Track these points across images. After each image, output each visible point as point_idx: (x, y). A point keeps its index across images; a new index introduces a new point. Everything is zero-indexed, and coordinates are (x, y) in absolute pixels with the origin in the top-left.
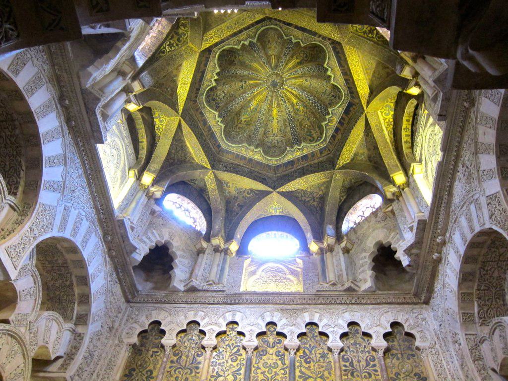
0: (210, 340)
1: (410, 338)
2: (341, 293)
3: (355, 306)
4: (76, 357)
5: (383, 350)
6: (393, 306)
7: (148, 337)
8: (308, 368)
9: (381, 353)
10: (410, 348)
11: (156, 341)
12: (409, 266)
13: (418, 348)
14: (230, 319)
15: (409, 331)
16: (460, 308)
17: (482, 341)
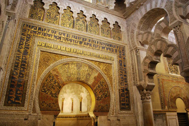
0: (61, 11)
1: (119, 27)
2: (104, 8)
3: (107, 13)
4: (17, 6)
5: (112, 29)
6: (117, 17)
7: (37, 3)
8: (92, 28)
9: (111, 29)
10: (118, 30)
11: (41, 6)
12: (128, 7)
13: (120, 31)
14: (68, 5)
15: (120, 25)
16: (139, 25)
17: (139, 34)
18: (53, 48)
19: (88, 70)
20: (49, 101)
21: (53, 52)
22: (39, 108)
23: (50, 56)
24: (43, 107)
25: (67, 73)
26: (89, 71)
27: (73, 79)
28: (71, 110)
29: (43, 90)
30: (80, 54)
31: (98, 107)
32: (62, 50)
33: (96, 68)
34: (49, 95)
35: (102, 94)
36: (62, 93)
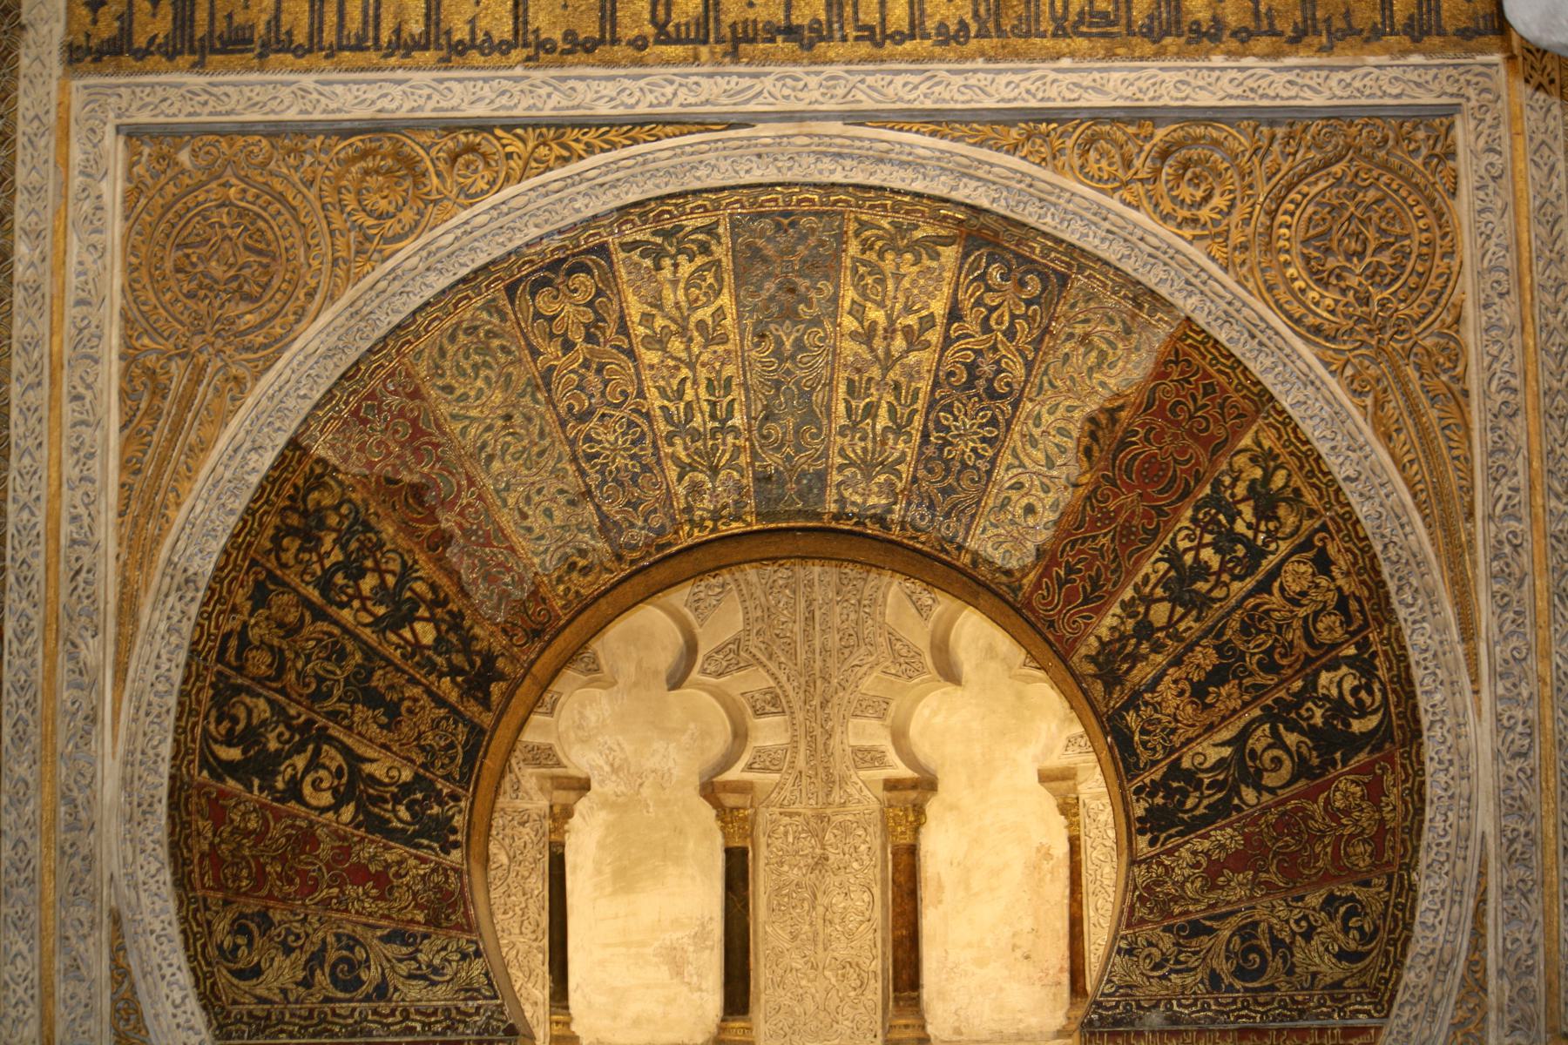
18: (300, 38)
19: (954, 314)
20: (325, 903)
21: (316, 116)
22: (199, 1020)
23: (278, 185)
24: (261, 1000)
25: (585, 416)
26: (986, 328)
27: (689, 509)
28: (1065, 978)
29: (235, 754)
30: (791, 32)
31: (1167, 942)
32: (461, 33)
33: (1111, 252)
34: (330, 815)
35: (1257, 712)
36: (870, 684)
